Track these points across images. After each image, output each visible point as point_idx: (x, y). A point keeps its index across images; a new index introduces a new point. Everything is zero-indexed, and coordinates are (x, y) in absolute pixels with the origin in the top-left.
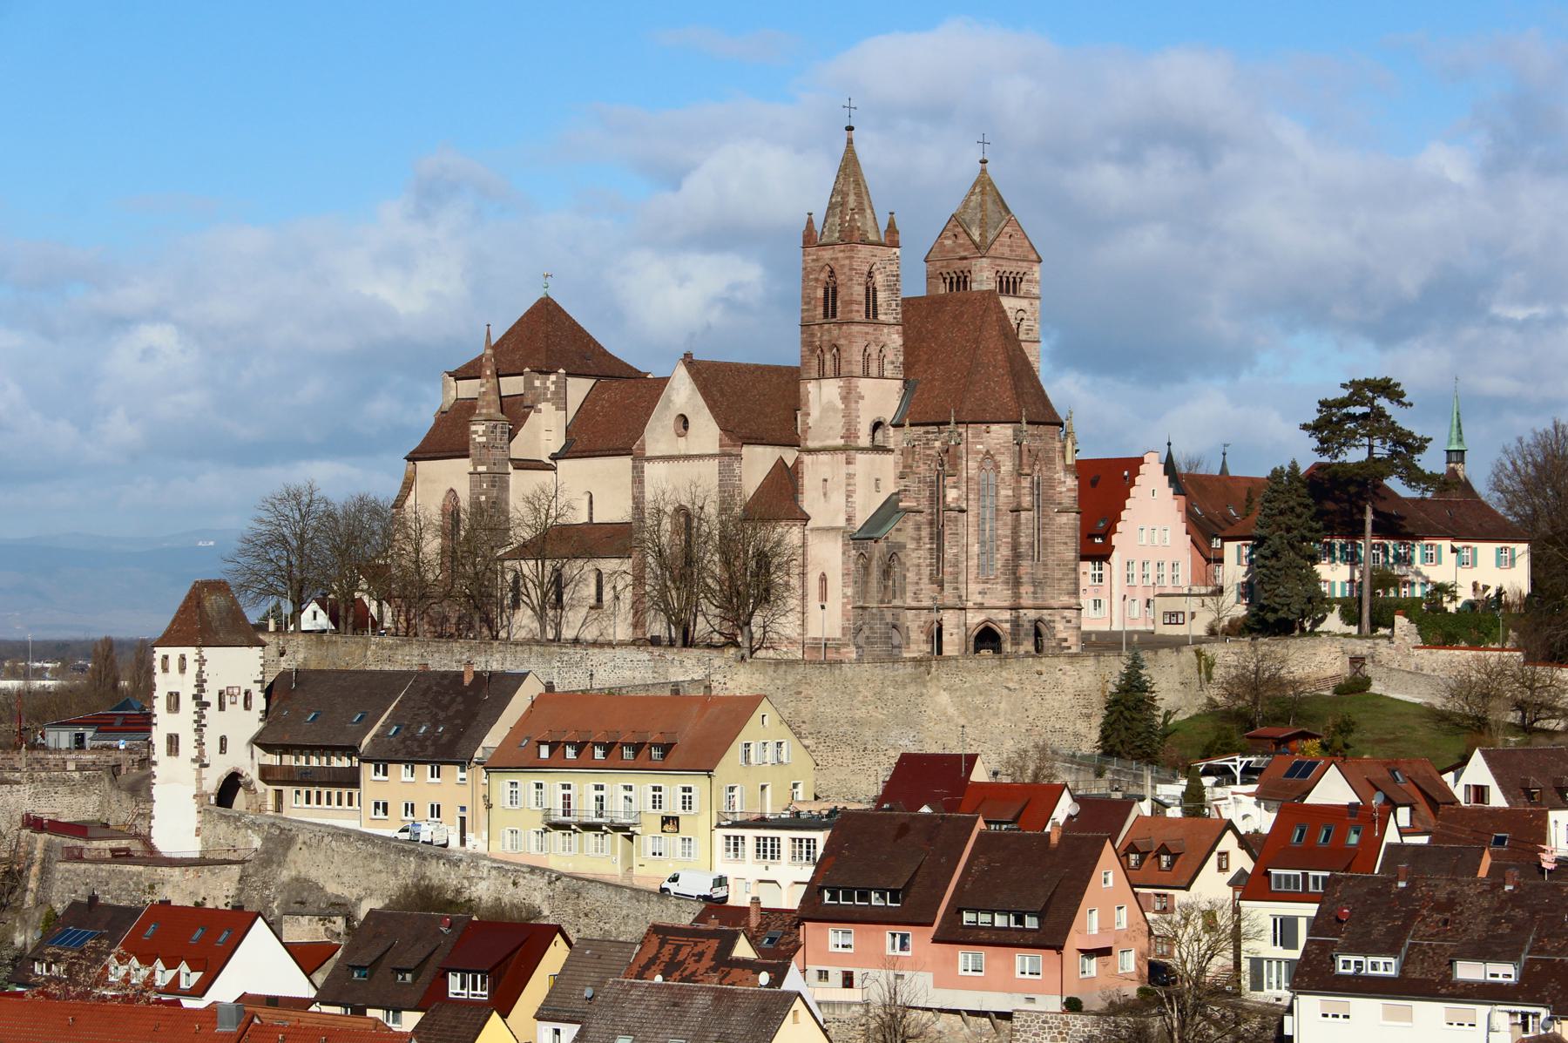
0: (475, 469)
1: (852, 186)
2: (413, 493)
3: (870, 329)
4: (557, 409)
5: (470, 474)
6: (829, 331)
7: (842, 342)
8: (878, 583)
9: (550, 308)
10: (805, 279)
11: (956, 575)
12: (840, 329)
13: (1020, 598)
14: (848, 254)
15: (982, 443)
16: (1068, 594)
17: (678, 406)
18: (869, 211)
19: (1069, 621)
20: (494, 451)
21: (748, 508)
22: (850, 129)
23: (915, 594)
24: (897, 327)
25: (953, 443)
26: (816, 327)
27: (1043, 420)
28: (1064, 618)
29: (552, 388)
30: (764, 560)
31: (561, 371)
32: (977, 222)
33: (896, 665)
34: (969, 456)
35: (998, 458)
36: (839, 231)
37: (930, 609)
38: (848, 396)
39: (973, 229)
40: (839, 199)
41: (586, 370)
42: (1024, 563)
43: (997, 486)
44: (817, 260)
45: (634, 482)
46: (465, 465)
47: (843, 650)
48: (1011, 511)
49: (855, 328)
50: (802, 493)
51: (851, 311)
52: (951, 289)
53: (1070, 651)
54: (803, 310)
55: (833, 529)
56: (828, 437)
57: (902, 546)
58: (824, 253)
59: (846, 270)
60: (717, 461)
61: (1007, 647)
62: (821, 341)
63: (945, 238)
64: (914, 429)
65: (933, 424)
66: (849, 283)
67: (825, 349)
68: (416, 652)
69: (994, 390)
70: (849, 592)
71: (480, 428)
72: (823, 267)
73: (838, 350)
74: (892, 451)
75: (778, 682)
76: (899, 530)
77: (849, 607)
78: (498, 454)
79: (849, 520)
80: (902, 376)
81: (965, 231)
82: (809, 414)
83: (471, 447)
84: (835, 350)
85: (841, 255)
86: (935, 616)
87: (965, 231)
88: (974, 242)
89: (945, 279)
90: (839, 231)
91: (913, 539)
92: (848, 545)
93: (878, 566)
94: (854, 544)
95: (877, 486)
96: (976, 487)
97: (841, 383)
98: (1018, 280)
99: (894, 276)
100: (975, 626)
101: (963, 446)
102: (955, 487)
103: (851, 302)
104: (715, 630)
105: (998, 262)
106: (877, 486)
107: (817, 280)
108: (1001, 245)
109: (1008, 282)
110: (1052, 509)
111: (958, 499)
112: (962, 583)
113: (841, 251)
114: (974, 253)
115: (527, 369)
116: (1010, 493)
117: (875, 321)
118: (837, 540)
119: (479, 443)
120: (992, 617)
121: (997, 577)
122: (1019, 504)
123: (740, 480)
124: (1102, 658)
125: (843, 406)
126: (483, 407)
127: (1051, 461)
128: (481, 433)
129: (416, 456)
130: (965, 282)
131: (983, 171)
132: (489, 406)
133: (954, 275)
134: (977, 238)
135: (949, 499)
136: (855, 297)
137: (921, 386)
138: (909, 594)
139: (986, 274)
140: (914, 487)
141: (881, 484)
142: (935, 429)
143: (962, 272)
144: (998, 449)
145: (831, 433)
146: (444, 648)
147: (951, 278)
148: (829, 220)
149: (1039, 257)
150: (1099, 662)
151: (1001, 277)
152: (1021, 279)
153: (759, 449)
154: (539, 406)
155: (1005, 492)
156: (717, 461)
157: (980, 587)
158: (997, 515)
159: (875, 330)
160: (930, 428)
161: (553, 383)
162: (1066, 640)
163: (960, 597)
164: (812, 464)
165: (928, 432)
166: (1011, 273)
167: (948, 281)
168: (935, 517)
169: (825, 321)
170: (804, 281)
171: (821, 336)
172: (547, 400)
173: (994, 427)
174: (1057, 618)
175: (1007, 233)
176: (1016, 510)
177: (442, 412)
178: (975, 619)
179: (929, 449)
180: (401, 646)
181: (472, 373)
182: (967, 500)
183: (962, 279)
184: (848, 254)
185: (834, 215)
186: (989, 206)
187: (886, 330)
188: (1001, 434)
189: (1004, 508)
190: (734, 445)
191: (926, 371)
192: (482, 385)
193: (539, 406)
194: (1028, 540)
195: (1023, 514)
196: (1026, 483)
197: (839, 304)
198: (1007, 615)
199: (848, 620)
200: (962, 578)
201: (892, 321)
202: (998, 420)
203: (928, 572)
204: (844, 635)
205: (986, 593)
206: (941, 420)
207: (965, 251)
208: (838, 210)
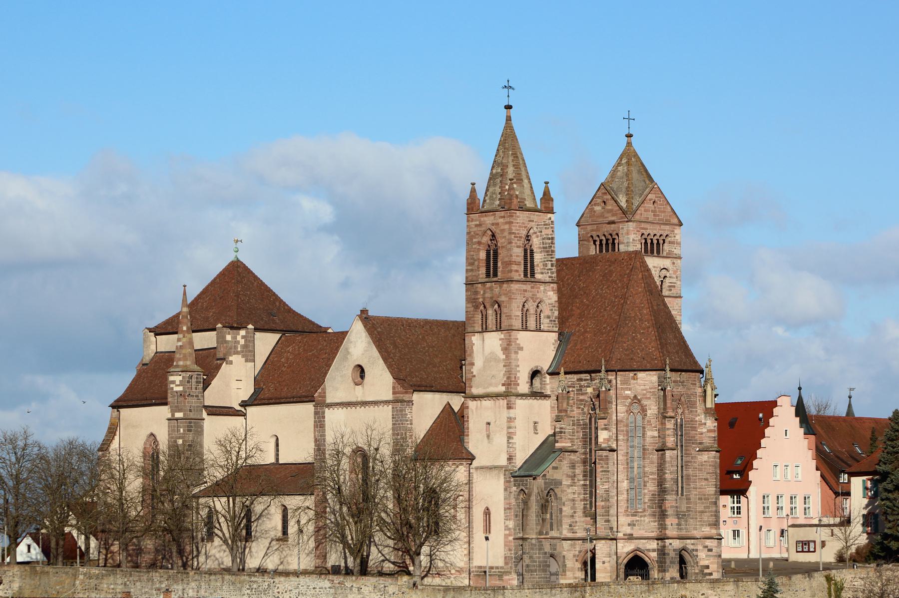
0: (173, 415)
1: (511, 158)
2: (117, 438)
3: (528, 287)
4: (246, 361)
5: (169, 419)
6: (491, 288)
7: (503, 298)
8: (537, 516)
9: (240, 270)
10: (469, 243)
11: (607, 509)
12: (501, 287)
13: (665, 529)
14: (508, 220)
15: (630, 389)
16: (710, 525)
17: (355, 357)
18: (526, 181)
19: (710, 550)
20: (189, 399)
21: (418, 448)
22: (508, 107)
23: (570, 526)
24: (552, 285)
25: (604, 389)
26: (480, 285)
27: (685, 368)
28: (706, 547)
29: (242, 342)
30: (433, 497)
31: (250, 326)
32: (624, 190)
33: (554, 591)
35: (644, 402)
36: (500, 199)
37: (584, 540)
38: (508, 348)
39: (621, 197)
40: (499, 170)
41: (273, 326)
42: (668, 497)
43: (644, 428)
44: (480, 225)
45: (315, 426)
46: (163, 412)
47: (505, 577)
48: (657, 451)
49: (515, 286)
50: (468, 435)
51: (511, 271)
52: (601, 251)
53: (712, 577)
54: (467, 270)
55: (496, 467)
56: (491, 385)
57: (559, 483)
58: (486, 219)
59: (506, 234)
60: (390, 407)
61: (655, 574)
62: (484, 298)
63: (595, 205)
64: (568, 376)
65: (586, 372)
66: (509, 246)
67: (488, 306)
68: (119, 581)
69: (640, 341)
70: (511, 524)
71: (177, 379)
72: (485, 232)
73: (499, 306)
74: (549, 396)
76: (555, 468)
77: (511, 538)
78: (193, 401)
79: (510, 459)
80: (557, 329)
81: (613, 198)
82: (473, 364)
83: (169, 395)
84: (496, 306)
85: (501, 220)
86: (589, 546)
87: (613, 198)
88: (621, 208)
89: (595, 242)
90: (500, 199)
91: (568, 476)
92: (510, 482)
93: (537, 501)
94: (515, 481)
95: (535, 429)
96: (625, 429)
97: (502, 336)
98: (661, 242)
99: (549, 239)
100: (625, 555)
101: (612, 392)
102: (606, 429)
103: (510, 263)
104: (387, 560)
105: (643, 225)
106: (535, 429)
107: (479, 243)
108: (645, 211)
109: (652, 243)
110: (694, 448)
111: (608, 440)
112: (612, 516)
113: (502, 217)
114: (622, 218)
115: (219, 325)
116: (656, 434)
117: (533, 280)
118: (499, 477)
119: (177, 392)
120: (640, 546)
121: (644, 510)
122: (664, 444)
123: (411, 424)
124: (741, 584)
125: (504, 357)
126: (179, 360)
127: (691, 405)
128: (178, 383)
129: (120, 403)
130: (613, 244)
131: (629, 144)
132: (185, 358)
133: (603, 238)
134: (623, 204)
135: (600, 440)
136: (514, 258)
137: (575, 338)
138: (565, 526)
139: (632, 237)
140: (569, 429)
141: (539, 427)
142: (587, 376)
143: (611, 235)
144: (644, 395)
145: (493, 381)
146: (145, 577)
147: (601, 241)
148: (491, 190)
149: (680, 221)
150: (738, 586)
151: (646, 239)
152: (664, 240)
153: (429, 396)
154: (231, 358)
155: (652, 433)
156: (390, 407)
157: (629, 519)
158: (644, 454)
159: (532, 288)
160: (583, 376)
161: (243, 337)
162: (707, 567)
163: (611, 528)
165: (581, 380)
166: (655, 235)
167: (598, 243)
168: (588, 456)
169: (487, 280)
170: (468, 244)
171: (484, 293)
172: (237, 353)
173: (641, 375)
174: (700, 547)
175: (650, 200)
176: (661, 450)
177: (143, 365)
178: (626, 548)
179: (582, 394)
180: (106, 575)
181: (170, 329)
182: (617, 440)
183: (610, 241)
184: (508, 220)
185: (495, 185)
186: (635, 175)
187: (542, 288)
188: (647, 380)
189: (650, 448)
190: (406, 393)
191: (578, 325)
192: (179, 340)
193: (231, 358)
194: (672, 476)
195: (668, 453)
196: (670, 425)
197: (499, 264)
198: (654, 545)
199: (510, 550)
200: (613, 511)
201: (548, 279)
202: (644, 368)
203: (582, 507)
204: (506, 563)
205: (634, 525)
206: (592, 368)
207: (613, 215)
208: (498, 180)
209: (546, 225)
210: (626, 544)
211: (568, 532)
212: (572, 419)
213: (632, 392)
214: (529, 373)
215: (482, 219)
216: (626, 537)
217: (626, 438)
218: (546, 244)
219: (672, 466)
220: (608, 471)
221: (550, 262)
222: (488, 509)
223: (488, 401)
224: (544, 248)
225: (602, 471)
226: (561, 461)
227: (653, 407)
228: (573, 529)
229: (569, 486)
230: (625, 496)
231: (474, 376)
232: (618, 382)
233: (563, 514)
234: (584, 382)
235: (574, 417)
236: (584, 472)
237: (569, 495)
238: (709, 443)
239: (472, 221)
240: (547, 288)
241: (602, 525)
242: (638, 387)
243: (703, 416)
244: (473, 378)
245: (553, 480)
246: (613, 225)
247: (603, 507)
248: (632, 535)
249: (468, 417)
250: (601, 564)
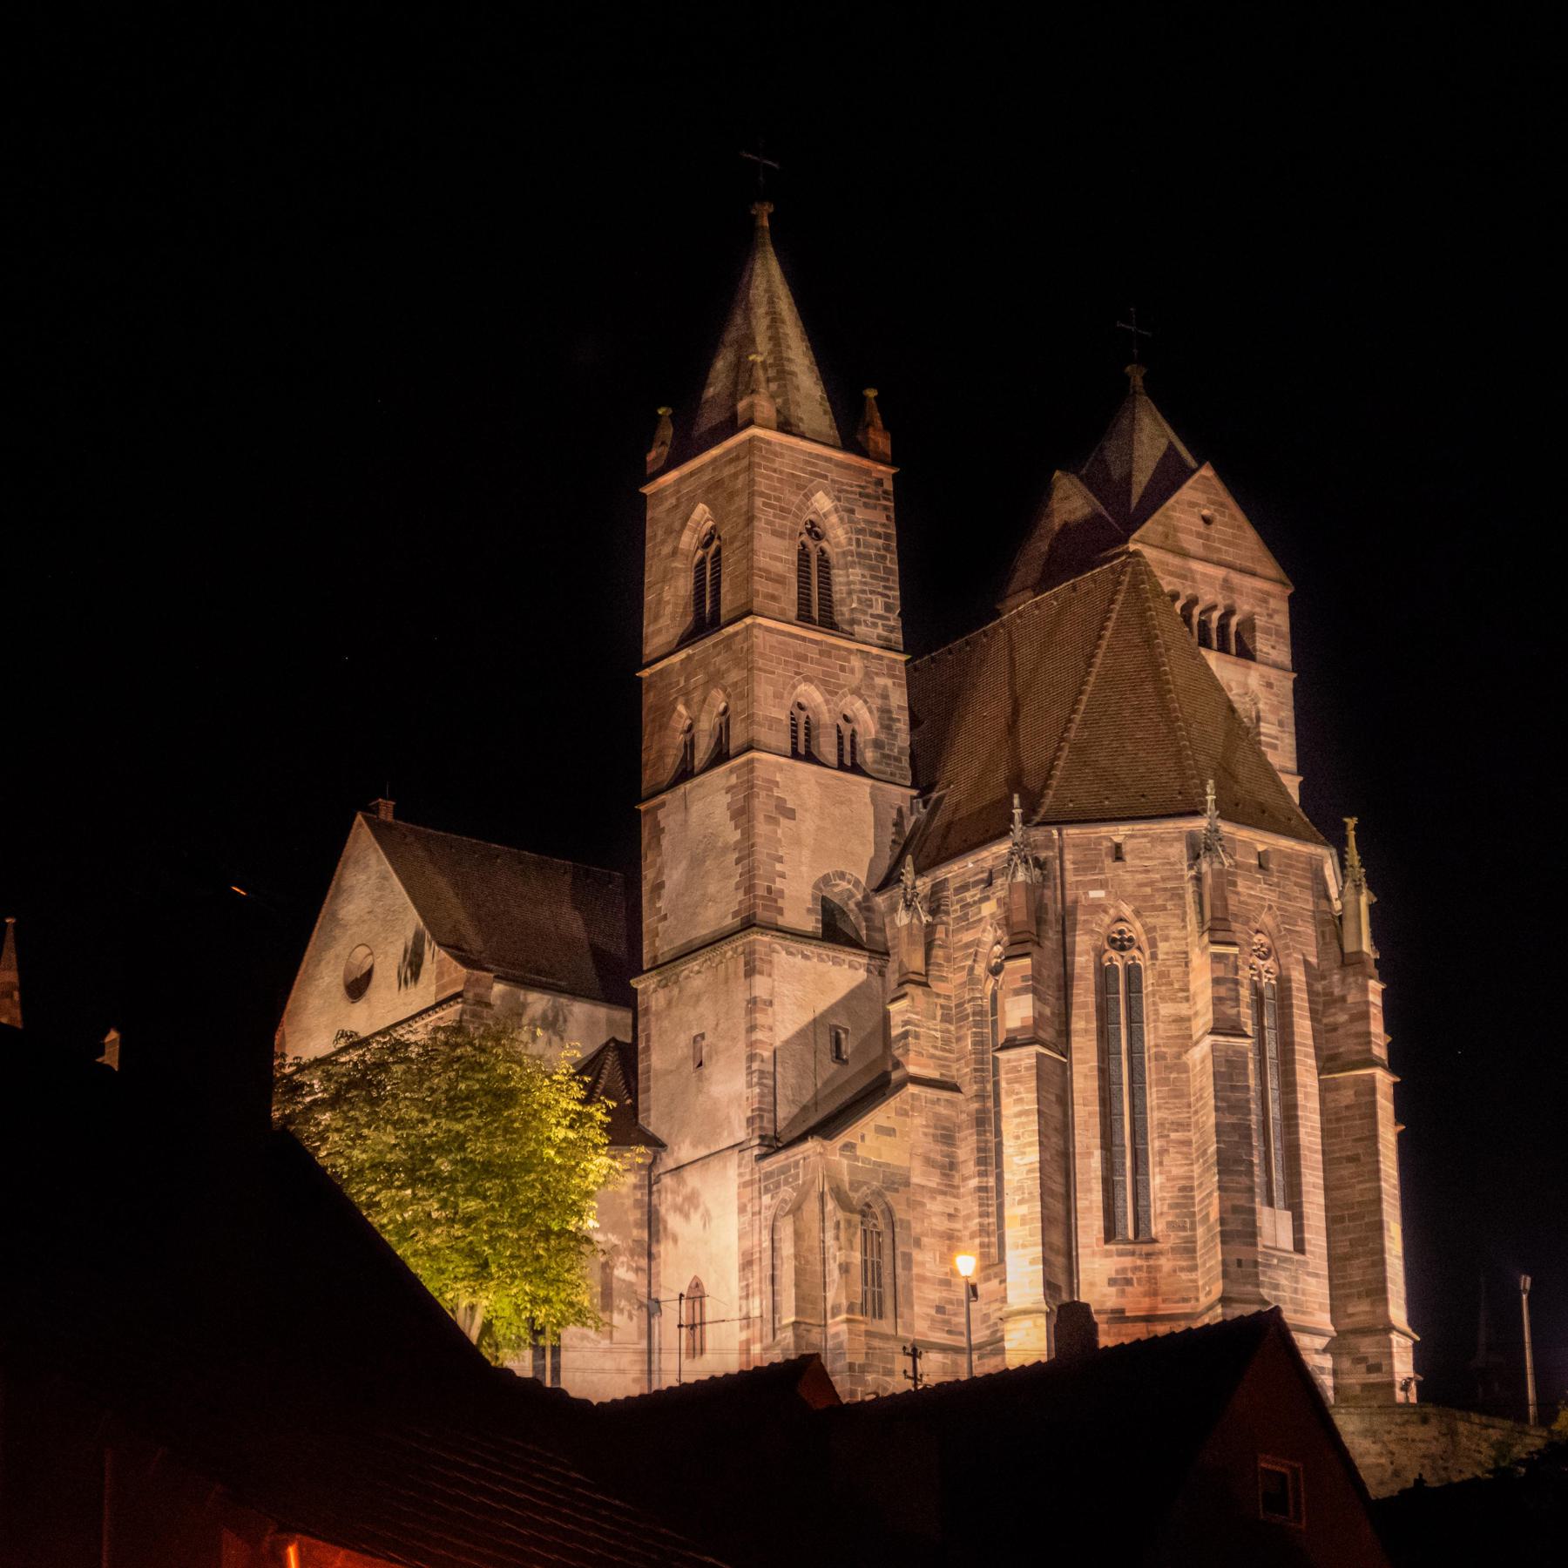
15: (1102, 885)
23: (940, 1309)
28: (1363, 1360)
50: (648, 1090)
91: (928, 1161)
168: (990, 1104)
209: (868, 496)
211: (932, 1328)
212: (942, 1001)
213: (1109, 893)
218: (867, 546)
221: (880, 599)
222: (697, 1285)
224: (859, 555)
225: (1020, 1114)
226: (905, 1114)
227: (1174, 933)
228: (948, 1322)
229: (933, 1193)
232: (1068, 866)
233: (915, 1270)
234: (972, 892)
235: (948, 997)
236: (979, 1150)
237: (934, 1220)
238: (1358, 1052)
242: (1127, 877)
245: (880, 1165)
248: (1122, 1311)
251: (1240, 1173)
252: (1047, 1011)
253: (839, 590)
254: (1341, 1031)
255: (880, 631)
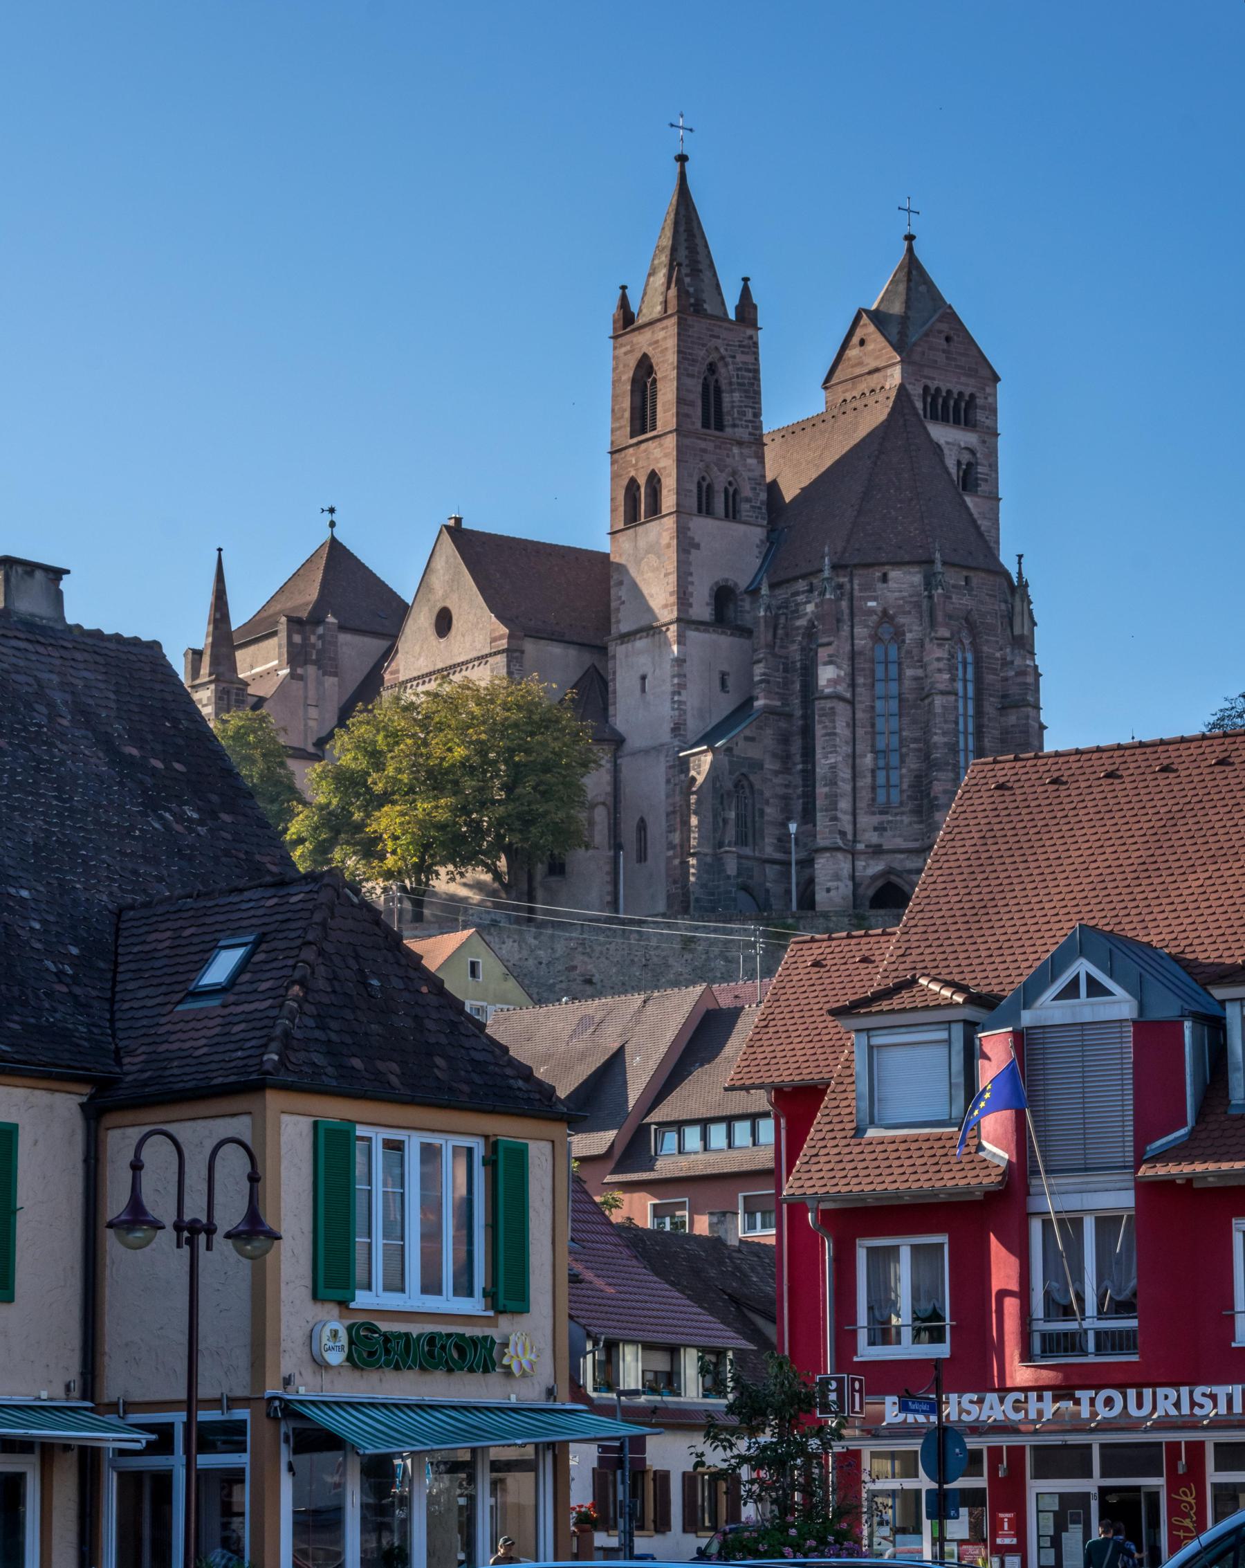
15: (874, 599)
23: (780, 840)
26: (631, 450)
34: (856, 619)
35: (901, 620)
43: (900, 664)
50: (615, 703)
57: (759, 766)
75: (541, 953)
85: (662, 334)
91: (774, 755)
96: (867, 666)
100: (866, 882)
102: (830, 663)
105: (927, 372)
120: (896, 865)
128: (205, 702)
131: (910, 250)
135: (822, 682)
141: (730, 681)
144: (899, 606)
157: (876, 819)
164: (627, 656)
173: (894, 574)
175: (940, 332)
194: (946, 740)
199: (675, 882)
200: (844, 804)
203: (800, 808)
205: (885, 829)
207: (877, 358)
209: (744, 346)
210: (871, 862)
214: (711, 589)
215: (635, 340)
216: (870, 850)
217: (869, 681)
218: (743, 377)
219: (946, 722)
220: (835, 734)
223: (645, 640)
225: (827, 734)
226: (760, 728)
227: (915, 628)
229: (776, 773)
230: (869, 780)
231: (623, 603)
232: (856, 587)
233: (766, 818)
239: (622, 345)
240: (746, 451)
241: (826, 827)
243: (1008, 650)
244: (622, 607)
246: (876, 375)
247: (827, 796)
248: (881, 846)
249: (614, 673)
250: (824, 894)
251: (947, 771)
252: (842, 673)
253: (726, 406)
254: (1010, 682)
255: (750, 429)
